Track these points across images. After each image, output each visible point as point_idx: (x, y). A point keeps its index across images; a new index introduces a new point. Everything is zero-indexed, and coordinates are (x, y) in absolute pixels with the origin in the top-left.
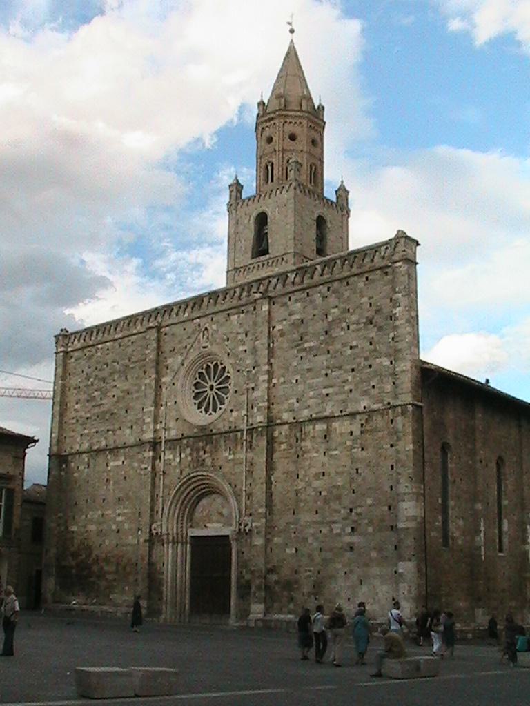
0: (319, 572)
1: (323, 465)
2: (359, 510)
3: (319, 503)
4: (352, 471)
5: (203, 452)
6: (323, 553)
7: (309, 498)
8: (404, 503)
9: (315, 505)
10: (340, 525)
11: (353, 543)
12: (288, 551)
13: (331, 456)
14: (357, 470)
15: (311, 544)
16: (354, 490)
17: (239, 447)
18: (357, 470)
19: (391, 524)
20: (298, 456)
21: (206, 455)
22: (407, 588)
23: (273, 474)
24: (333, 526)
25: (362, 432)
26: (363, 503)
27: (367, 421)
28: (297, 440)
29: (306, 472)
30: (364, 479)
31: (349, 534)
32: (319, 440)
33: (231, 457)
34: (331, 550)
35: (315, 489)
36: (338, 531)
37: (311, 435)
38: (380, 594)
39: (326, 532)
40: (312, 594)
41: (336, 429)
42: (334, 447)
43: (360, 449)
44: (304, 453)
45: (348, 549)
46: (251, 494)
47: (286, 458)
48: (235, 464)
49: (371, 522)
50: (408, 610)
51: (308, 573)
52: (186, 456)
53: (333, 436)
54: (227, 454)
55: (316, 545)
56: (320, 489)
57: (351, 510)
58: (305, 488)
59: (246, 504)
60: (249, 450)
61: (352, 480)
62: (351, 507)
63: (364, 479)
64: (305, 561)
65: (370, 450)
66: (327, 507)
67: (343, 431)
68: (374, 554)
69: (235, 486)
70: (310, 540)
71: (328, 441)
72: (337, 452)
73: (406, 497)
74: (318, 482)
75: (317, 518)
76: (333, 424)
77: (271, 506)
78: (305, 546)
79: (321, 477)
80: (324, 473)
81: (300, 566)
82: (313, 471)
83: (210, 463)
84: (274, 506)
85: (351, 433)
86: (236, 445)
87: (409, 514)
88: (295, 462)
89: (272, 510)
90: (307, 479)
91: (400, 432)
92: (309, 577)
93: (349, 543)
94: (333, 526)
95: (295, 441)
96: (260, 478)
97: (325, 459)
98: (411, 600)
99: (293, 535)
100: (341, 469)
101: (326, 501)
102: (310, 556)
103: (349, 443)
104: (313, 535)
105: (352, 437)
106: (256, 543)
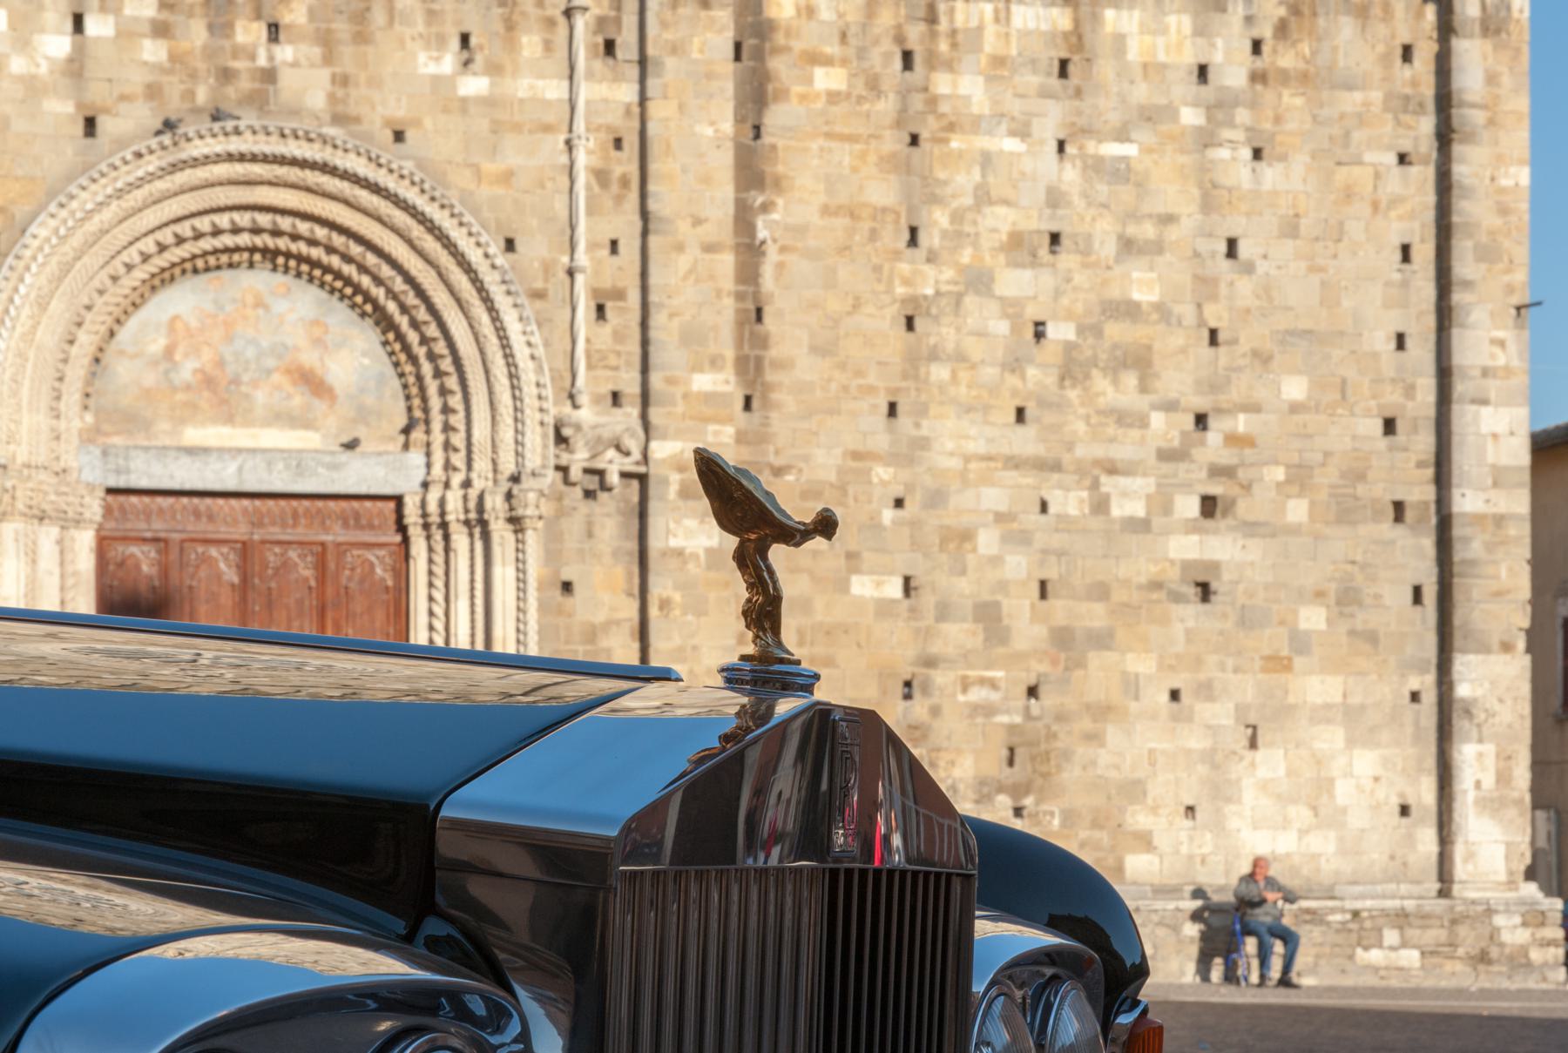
0: (1032, 692)
1: (1055, 199)
2: (1241, 423)
3: (1032, 372)
4: (1203, 246)
5: (260, 30)
6: (1059, 608)
7: (974, 348)
8: (1485, 411)
9: (1012, 381)
10: (1142, 485)
11: (1214, 566)
12: (862, 586)
13: (1096, 167)
14: (1232, 245)
15: (996, 561)
16: (1213, 334)
17: (530, 43)
18: (1232, 245)
19: (1398, 497)
20: (914, 140)
21: (285, 52)
22: (1490, 762)
23: (766, 208)
24: (1108, 484)
25: (1258, 77)
26: (1261, 394)
27: (1282, 29)
28: (907, 59)
29: (957, 217)
30: (1266, 291)
31: (1191, 528)
32: (1031, 80)
33: (474, 85)
34: (1100, 592)
35: (1011, 309)
36: (1138, 509)
37: (990, 43)
38: (1343, 791)
39: (1073, 510)
40: (1001, 789)
41: (1120, 39)
42: (1114, 118)
43: (1246, 153)
44: (951, 127)
45: (1192, 592)
46: (619, 295)
47: (851, 139)
48: (497, 128)
49: (1299, 478)
50: (1500, 851)
51: (977, 695)
52: (126, 35)
53: (1105, 69)
54: (448, 62)
55: (1018, 566)
56: (1032, 312)
57: (1201, 420)
58: (958, 299)
59: (588, 341)
60: (599, 65)
61: (1206, 287)
62: (1201, 403)
63: (1266, 291)
64: (958, 635)
65: (1300, 161)
66: (1073, 394)
67: (1162, 57)
68: (1313, 618)
69: (510, 245)
70: (987, 541)
71: (1078, 93)
72: (1130, 150)
73: (1493, 387)
74: (1027, 274)
75: (1025, 441)
76: (1109, 14)
77: (759, 362)
78: (963, 572)
79: (1044, 252)
80: (1055, 238)
81: (930, 662)
82: (999, 221)
83: (317, 100)
84: (779, 365)
85: (1203, 72)
86: (510, 26)
87: (1505, 460)
88: (906, 168)
89: (767, 388)
90: (966, 256)
91: (1474, 106)
92: (988, 710)
93: (1187, 566)
94: (1108, 484)
95: (898, 63)
96: (697, 222)
97: (1070, 175)
98: (1512, 812)
99: (888, 515)
100: (1148, 231)
101: (1072, 370)
102: (989, 616)
103: (1190, 117)
104: (1000, 518)
105: (1207, 92)
106: (674, 543)
